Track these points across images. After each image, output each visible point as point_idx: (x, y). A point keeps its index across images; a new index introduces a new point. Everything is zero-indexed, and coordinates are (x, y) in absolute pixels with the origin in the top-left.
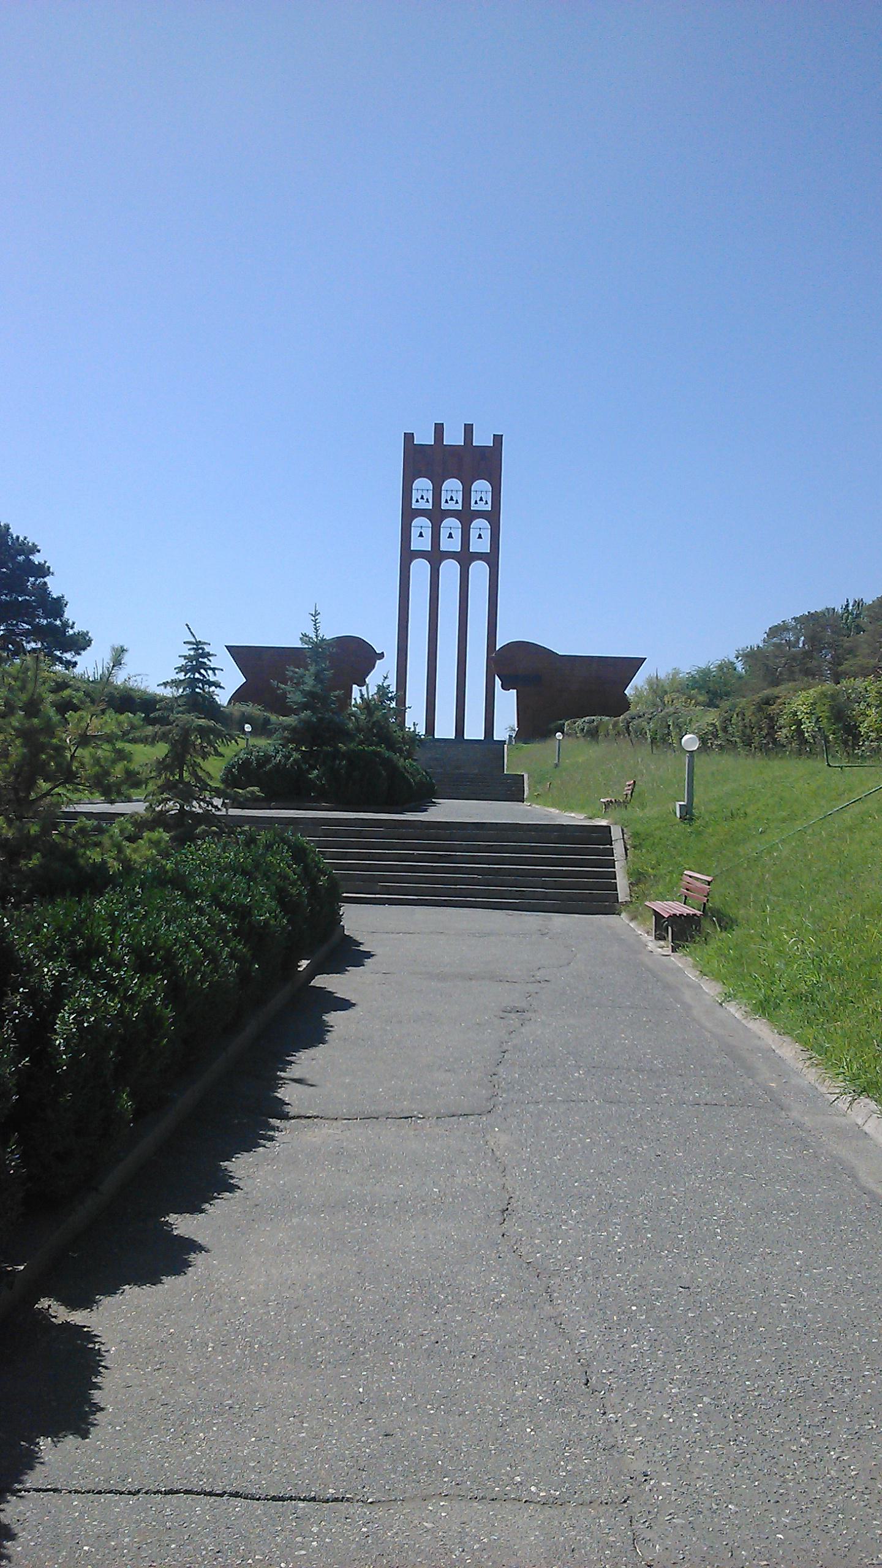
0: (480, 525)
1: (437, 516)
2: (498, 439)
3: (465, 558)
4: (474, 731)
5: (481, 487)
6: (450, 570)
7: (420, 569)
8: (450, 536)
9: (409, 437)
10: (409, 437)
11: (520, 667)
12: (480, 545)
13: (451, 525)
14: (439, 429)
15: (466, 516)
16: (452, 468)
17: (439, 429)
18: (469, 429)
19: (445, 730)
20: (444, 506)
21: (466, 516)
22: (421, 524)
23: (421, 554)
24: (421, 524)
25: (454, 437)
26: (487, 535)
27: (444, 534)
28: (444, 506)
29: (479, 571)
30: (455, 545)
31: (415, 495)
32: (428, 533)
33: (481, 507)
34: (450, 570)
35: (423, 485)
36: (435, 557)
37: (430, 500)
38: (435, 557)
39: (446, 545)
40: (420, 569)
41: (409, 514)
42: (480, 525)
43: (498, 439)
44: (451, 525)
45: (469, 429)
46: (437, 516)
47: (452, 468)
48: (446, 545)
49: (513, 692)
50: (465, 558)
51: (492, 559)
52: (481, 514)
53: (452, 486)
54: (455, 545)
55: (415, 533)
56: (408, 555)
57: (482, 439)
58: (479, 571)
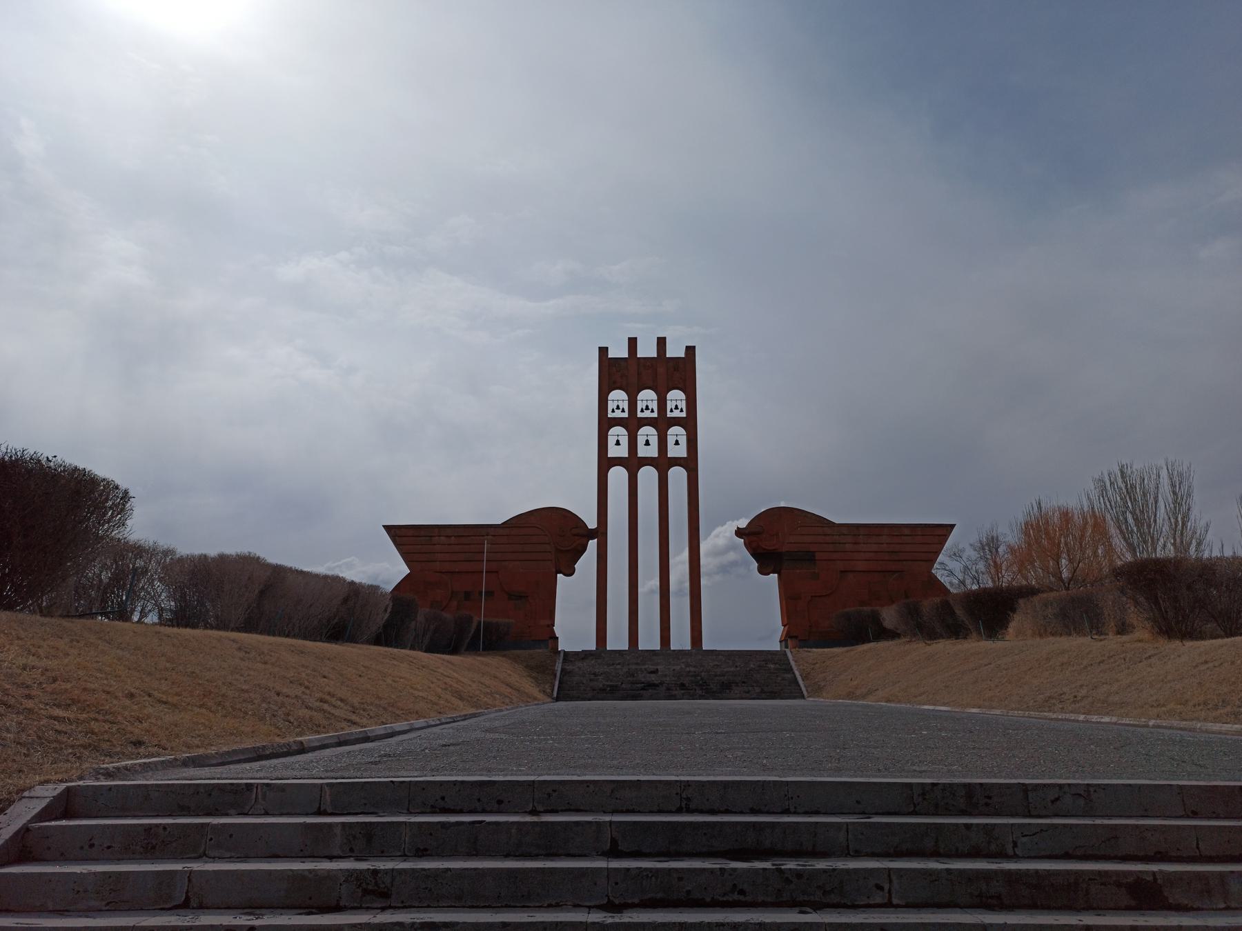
0: (676, 433)
1: (633, 424)
2: (691, 350)
3: (663, 463)
4: (681, 640)
5: (676, 397)
6: (647, 476)
7: (618, 476)
8: (647, 443)
9: (603, 351)
10: (603, 351)
11: (778, 540)
12: (677, 450)
13: (647, 432)
14: (633, 342)
15: (662, 423)
16: (648, 379)
17: (633, 342)
18: (662, 342)
19: (649, 640)
20: (640, 415)
21: (662, 423)
22: (618, 432)
23: (618, 461)
24: (618, 432)
25: (647, 350)
26: (683, 440)
27: (641, 440)
28: (640, 415)
29: (678, 476)
30: (652, 451)
31: (611, 405)
32: (625, 441)
33: (677, 414)
34: (647, 476)
35: (618, 398)
36: (633, 463)
37: (626, 409)
38: (633, 463)
39: (643, 452)
40: (618, 476)
41: (606, 423)
42: (676, 433)
43: (691, 350)
44: (647, 432)
45: (662, 342)
46: (633, 424)
47: (648, 379)
48: (643, 452)
49: (774, 577)
50: (663, 463)
51: (690, 463)
52: (676, 422)
53: (647, 397)
54: (652, 451)
55: (611, 441)
56: (605, 463)
57: (675, 351)
58: (678, 476)
